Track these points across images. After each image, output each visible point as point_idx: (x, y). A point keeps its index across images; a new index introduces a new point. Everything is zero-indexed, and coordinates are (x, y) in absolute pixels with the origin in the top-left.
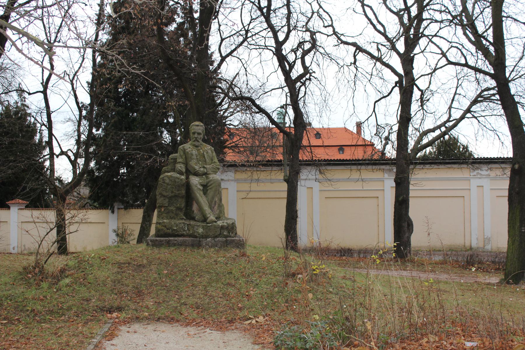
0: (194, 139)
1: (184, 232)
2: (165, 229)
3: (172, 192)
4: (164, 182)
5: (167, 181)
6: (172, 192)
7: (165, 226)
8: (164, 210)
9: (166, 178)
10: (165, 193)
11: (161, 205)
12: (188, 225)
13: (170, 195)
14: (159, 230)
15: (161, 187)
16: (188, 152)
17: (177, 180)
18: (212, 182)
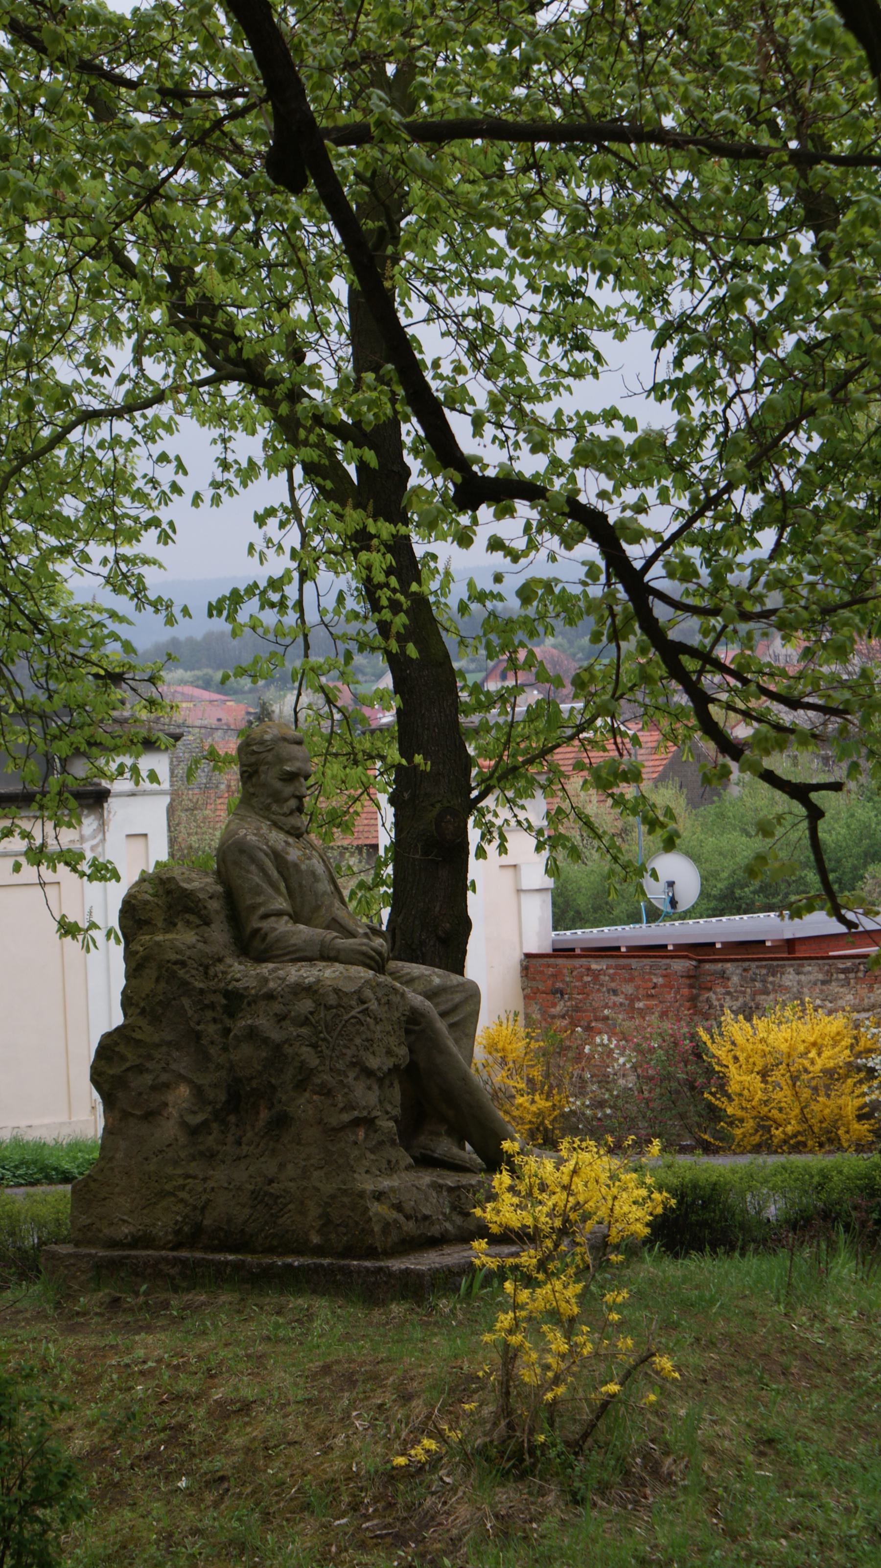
0: (293, 803)
1: (448, 1225)
2: (401, 1218)
3: (389, 1053)
4: (365, 1012)
5: (373, 1005)
6: (389, 1053)
7: (398, 1207)
8: (367, 1135)
9: (368, 993)
10: (373, 1063)
11: (365, 1113)
12: (451, 1190)
13: (385, 1068)
14: (388, 1224)
15: (358, 1033)
16: (296, 865)
17: (395, 999)
18: (458, 998)
